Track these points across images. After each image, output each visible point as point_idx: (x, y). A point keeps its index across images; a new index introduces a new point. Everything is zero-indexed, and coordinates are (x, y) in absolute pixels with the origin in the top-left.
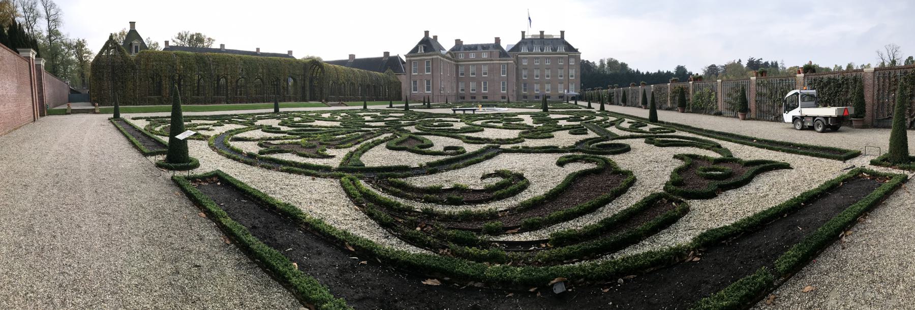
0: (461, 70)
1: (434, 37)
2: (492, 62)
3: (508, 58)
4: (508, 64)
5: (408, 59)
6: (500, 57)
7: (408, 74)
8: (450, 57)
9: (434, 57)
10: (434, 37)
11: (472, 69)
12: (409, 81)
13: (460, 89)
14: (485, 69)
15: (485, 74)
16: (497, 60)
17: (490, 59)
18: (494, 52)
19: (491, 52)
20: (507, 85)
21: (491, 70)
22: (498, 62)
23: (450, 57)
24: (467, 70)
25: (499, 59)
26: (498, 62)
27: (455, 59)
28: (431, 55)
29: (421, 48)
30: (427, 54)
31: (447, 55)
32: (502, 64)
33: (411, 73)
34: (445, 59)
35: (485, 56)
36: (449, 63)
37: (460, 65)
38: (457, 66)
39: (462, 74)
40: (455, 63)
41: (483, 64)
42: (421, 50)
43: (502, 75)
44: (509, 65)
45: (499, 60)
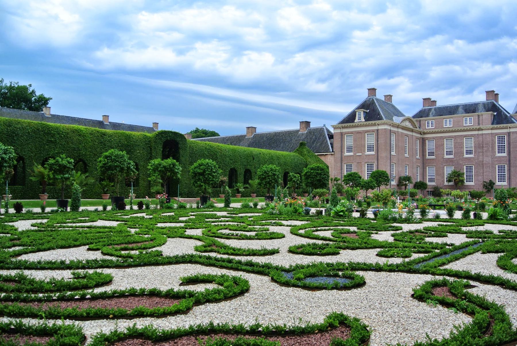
0: (430, 146)
1: (385, 96)
2: (480, 132)
3: (509, 125)
4: (509, 134)
5: (338, 131)
6: (492, 124)
7: (338, 155)
8: (411, 127)
9: (380, 127)
10: (385, 96)
11: (448, 145)
12: (339, 164)
13: (428, 178)
14: (469, 144)
15: (469, 152)
16: (488, 129)
17: (478, 127)
18: (484, 117)
19: (479, 116)
20: (509, 170)
21: (480, 146)
22: (490, 132)
23: (411, 127)
24: (439, 147)
25: (491, 126)
26: (490, 132)
27: (418, 129)
28: (375, 125)
29: (360, 114)
30: (368, 123)
31: (404, 124)
32: (496, 134)
33: (342, 152)
34: (400, 130)
35: (469, 121)
36: (407, 135)
37: (427, 138)
38: (423, 141)
39: (431, 154)
40: (419, 136)
41: (465, 136)
42: (360, 118)
43: (498, 155)
44: (512, 137)
45: (492, 129)
